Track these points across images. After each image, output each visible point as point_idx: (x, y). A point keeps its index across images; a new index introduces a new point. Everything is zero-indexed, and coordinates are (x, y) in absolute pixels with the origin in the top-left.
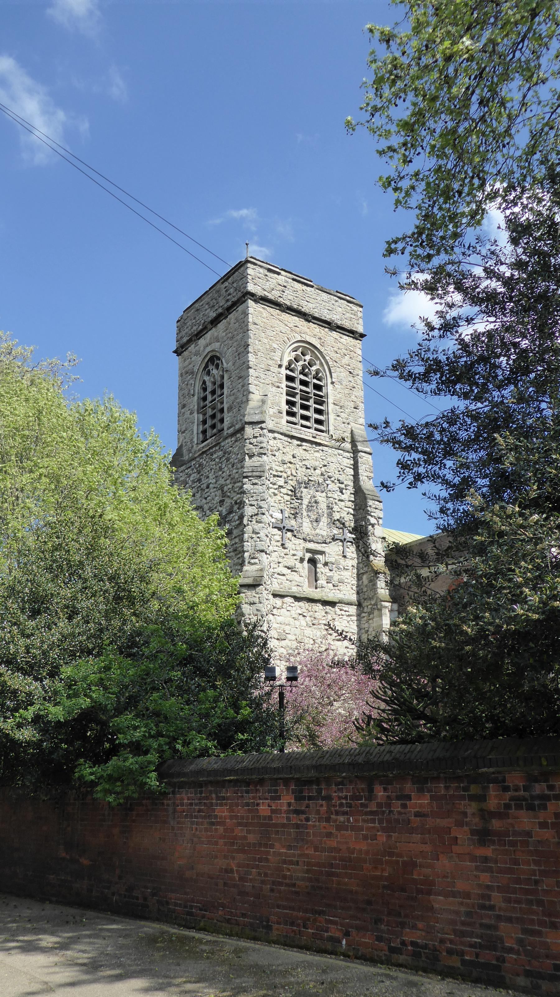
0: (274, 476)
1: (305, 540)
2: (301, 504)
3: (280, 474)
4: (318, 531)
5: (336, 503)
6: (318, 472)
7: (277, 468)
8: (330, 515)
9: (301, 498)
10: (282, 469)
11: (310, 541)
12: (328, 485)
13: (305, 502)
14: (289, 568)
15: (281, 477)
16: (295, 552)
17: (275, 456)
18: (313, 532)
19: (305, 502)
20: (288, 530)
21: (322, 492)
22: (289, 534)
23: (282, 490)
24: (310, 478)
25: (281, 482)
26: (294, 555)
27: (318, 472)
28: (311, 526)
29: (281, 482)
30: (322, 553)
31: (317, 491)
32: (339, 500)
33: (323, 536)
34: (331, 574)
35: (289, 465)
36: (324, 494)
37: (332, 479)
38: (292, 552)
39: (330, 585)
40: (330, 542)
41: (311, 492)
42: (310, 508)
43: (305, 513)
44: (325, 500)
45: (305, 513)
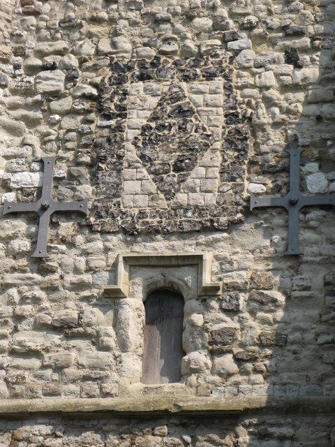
0: (32, 70)
1: (130, 234)
2: (119, 128)
3: (49, 59)
4: (182, 198)
5: (269, 102)
6: (204, 22)
7: (45, 46)
8: (234, 141)
9: (122, 112)
10: (61, 44)
11: (151, 233)
12: (237, 52)
13: (137, 119)
14: (53, 328)
15: (53, 67)
16: (87, 277)
17: (36, 14)
18: (163, 203)
19: (137, 119)
20: (67, 215)
21: (210, 76)
22: (67, 228)
23: (55, 105)
24: (167, 48)
25: (55, 80)
26: (79, 286)
27: (204, 22)
28: (153, 187)
29: (55, 80)
30: (195, 262)
31: (186, 79)
32: (285, 88)
33: (198, 210)
34: (231, 323)
35: (87, 28)
36: (219, 82)
37: (259, 30)
38: (71, 278)
39: (227, 362)
40: (232, 226)
41: (163, 87)
42: (149, 136)
43: (131, 153)
44: (220, 98)
45: (131, 153)
